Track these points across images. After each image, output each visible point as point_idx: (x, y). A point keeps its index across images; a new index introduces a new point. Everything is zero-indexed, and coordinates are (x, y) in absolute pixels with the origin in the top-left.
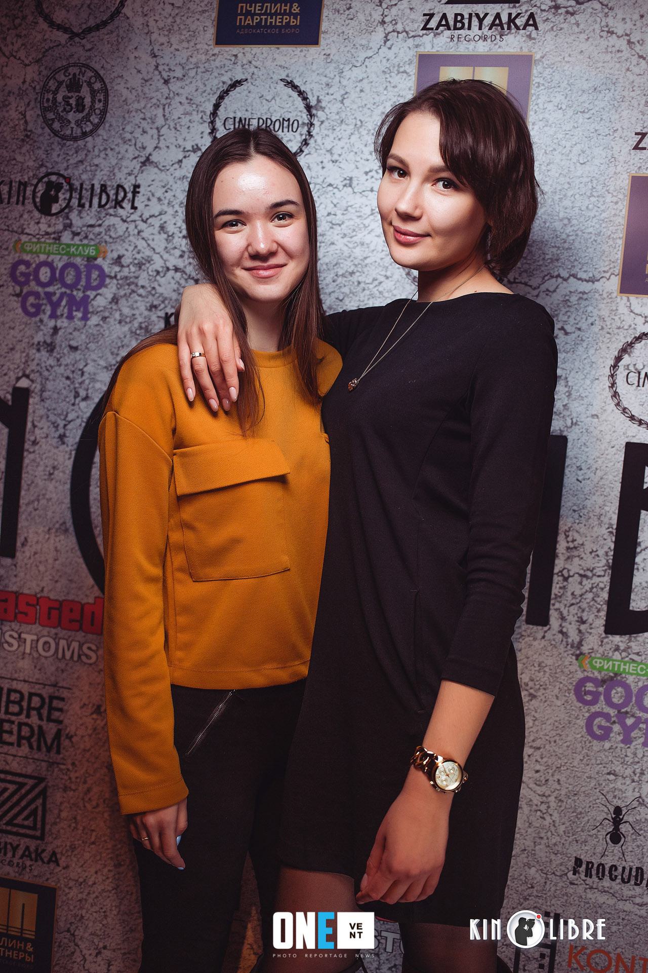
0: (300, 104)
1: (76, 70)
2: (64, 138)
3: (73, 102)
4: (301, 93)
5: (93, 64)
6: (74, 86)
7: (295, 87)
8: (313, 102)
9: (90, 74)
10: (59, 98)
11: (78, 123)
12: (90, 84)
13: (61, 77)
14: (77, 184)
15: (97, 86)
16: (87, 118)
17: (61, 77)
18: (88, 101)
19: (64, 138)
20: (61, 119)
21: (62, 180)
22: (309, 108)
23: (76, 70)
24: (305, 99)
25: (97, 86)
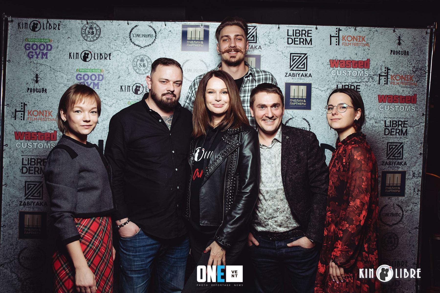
0: (205, 66)
1: (143, 57)
2: (140, 74)
3: (142, 65)
4: (205, 63)
5: (147, 55)
6: (142, 60)
7: (203, 61)
8: (208, 65)
9: (146, 57)
10: (138, 63)
11: (144, 70)
12: (147, 60)
13: (138, 58)
14: (145, 86)
15: (149, 60)
16: (146, 69)
17: (138, 58)
18: (146, 65)
19: (140, 74)
20: (139, 69)
21: (140, 85)
22: (207, 67)
23: (143, 57)
24: (206, 64)
25: (149, 60)
